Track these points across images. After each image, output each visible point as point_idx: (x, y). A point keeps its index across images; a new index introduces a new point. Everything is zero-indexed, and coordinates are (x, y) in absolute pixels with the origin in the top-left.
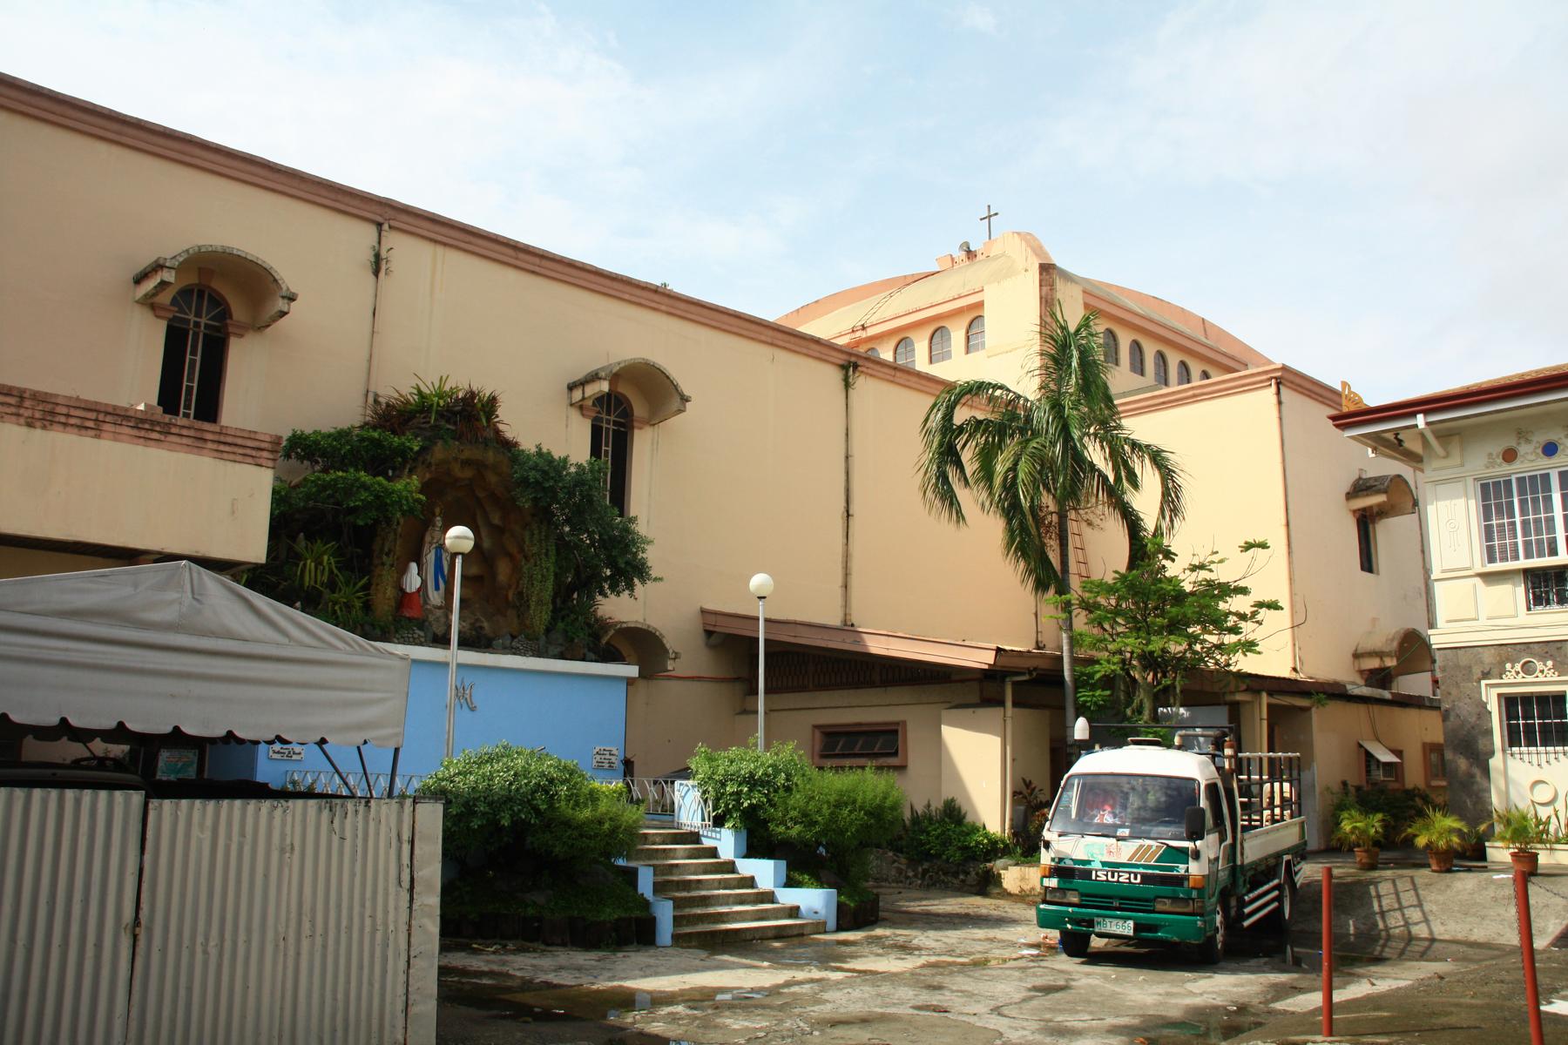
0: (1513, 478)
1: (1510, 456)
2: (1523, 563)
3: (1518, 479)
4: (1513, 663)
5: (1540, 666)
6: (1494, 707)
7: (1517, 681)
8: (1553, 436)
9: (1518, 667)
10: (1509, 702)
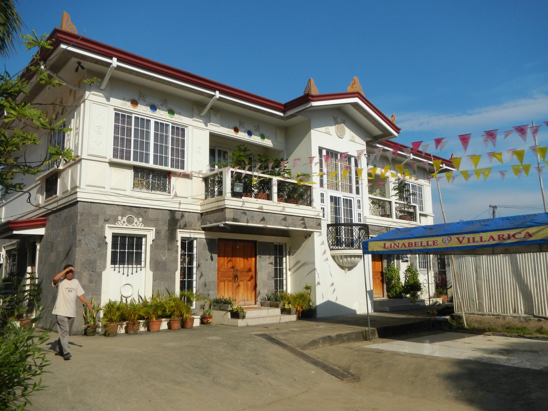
0: (133, 116)
1: (134, 103)
2: (132, 162)
3: (135, 117)
4: (123, 216)
5: (136, 220)
6: (109, 240)
7: (123, 227)
8: (156, 103)
9: (125, 219)
10: (115, 237)
